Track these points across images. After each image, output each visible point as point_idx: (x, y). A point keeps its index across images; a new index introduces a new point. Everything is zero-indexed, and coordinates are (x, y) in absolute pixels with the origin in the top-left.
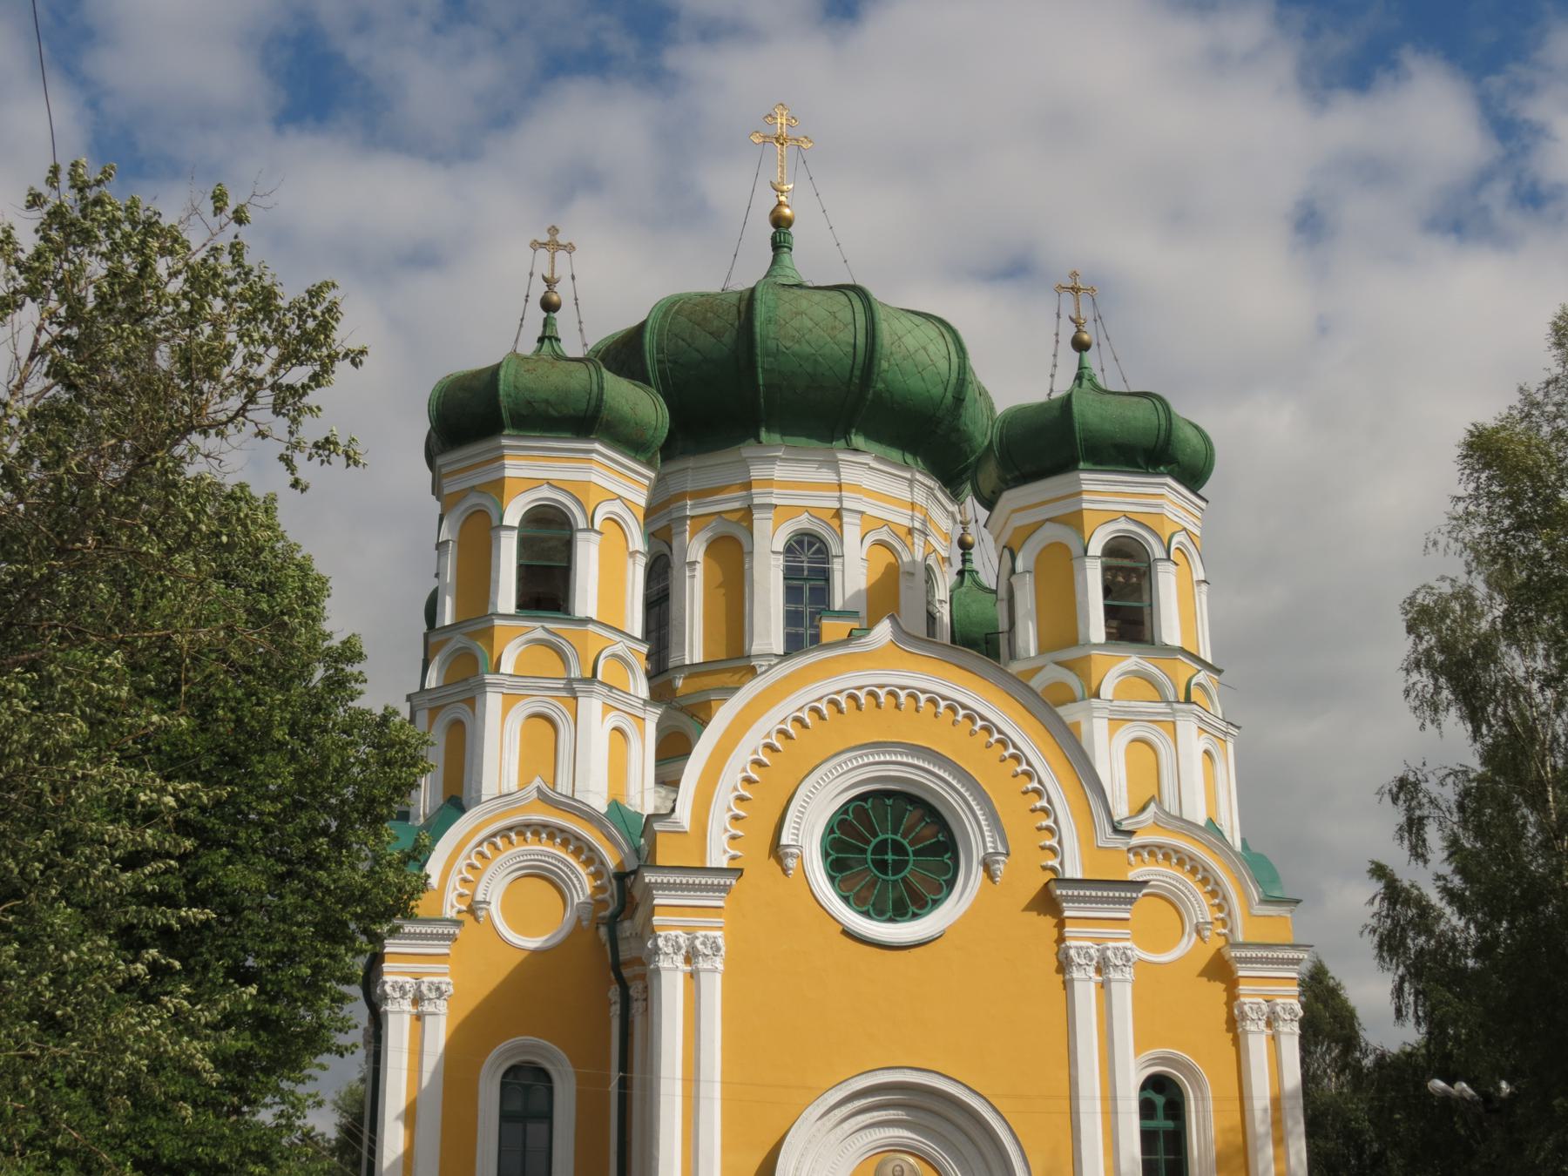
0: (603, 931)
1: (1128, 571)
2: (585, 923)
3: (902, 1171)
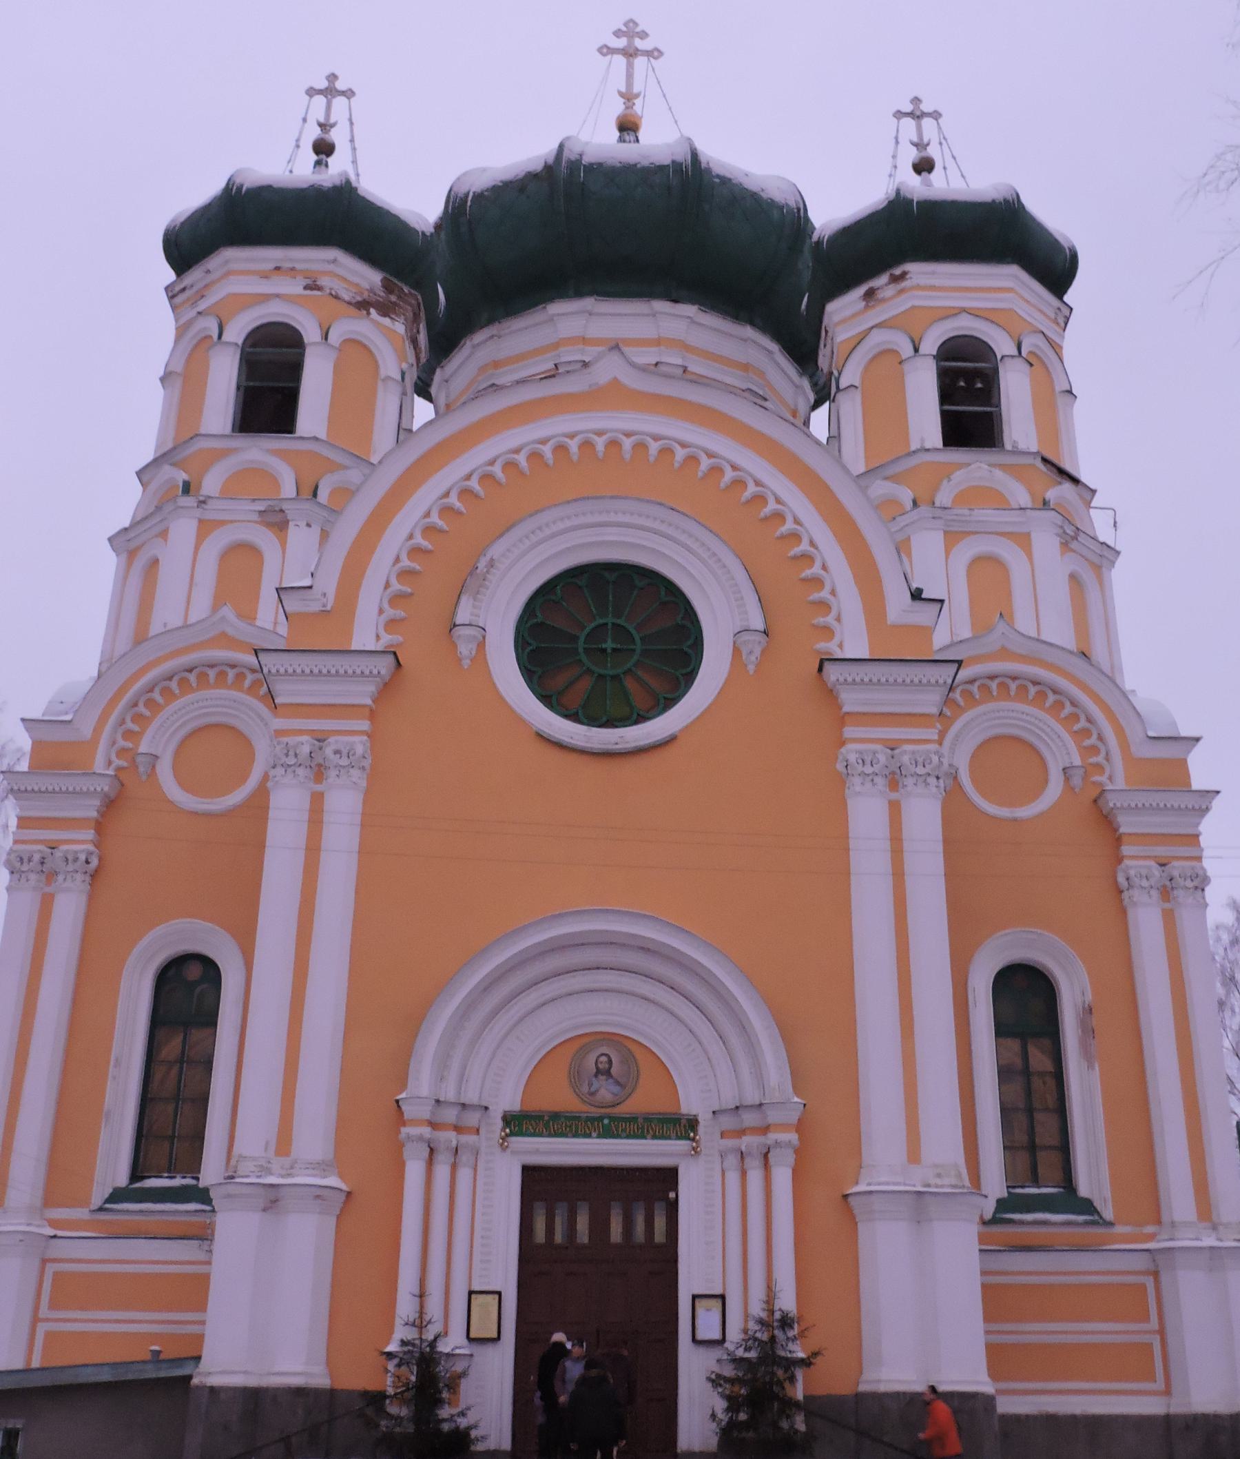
1: (971, 375)
3: (610, 1062)
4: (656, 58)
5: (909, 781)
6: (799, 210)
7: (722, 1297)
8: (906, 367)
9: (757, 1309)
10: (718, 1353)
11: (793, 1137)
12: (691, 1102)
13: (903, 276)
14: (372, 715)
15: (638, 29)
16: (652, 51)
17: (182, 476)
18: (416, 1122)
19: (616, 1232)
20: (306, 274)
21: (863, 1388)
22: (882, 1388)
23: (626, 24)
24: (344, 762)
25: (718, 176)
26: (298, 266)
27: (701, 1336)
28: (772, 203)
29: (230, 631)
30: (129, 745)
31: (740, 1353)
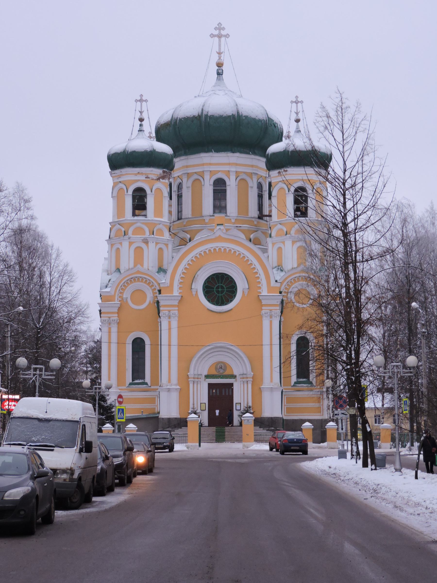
0: (156, 304)
1: (301, 196)
2: (151, 302)
4: (228, 38)
5: (274, 317)
6: (267, 120)
7: (240, 403)
8: (286, 195)
9: (246, 406)
10: (239, 412)
11: (252, 379)
12: (235, 373)
13: (286, 171)
14: (178, 306)
15: (222, 27)
16: (226, 35)
17: (123, 229)
18: (191, 378)
19: (223, 394)
20: (145, 174)
21: (262, 416)
22: (264, 416)
23: (218, 25)
24: (174, 316)
25: (245, 116)
26: (144, 172)
27: (237, 409)
28: (260, 121)
29: (139, 270)
30: (121, 295)
31: (243, 412)
